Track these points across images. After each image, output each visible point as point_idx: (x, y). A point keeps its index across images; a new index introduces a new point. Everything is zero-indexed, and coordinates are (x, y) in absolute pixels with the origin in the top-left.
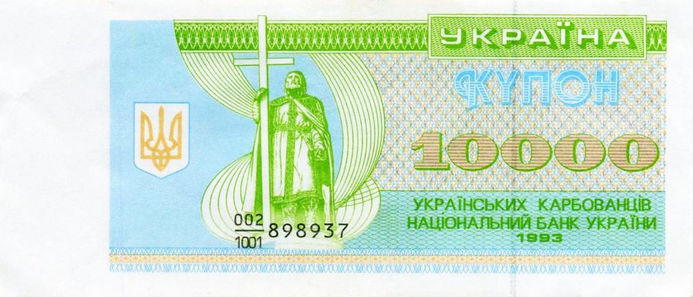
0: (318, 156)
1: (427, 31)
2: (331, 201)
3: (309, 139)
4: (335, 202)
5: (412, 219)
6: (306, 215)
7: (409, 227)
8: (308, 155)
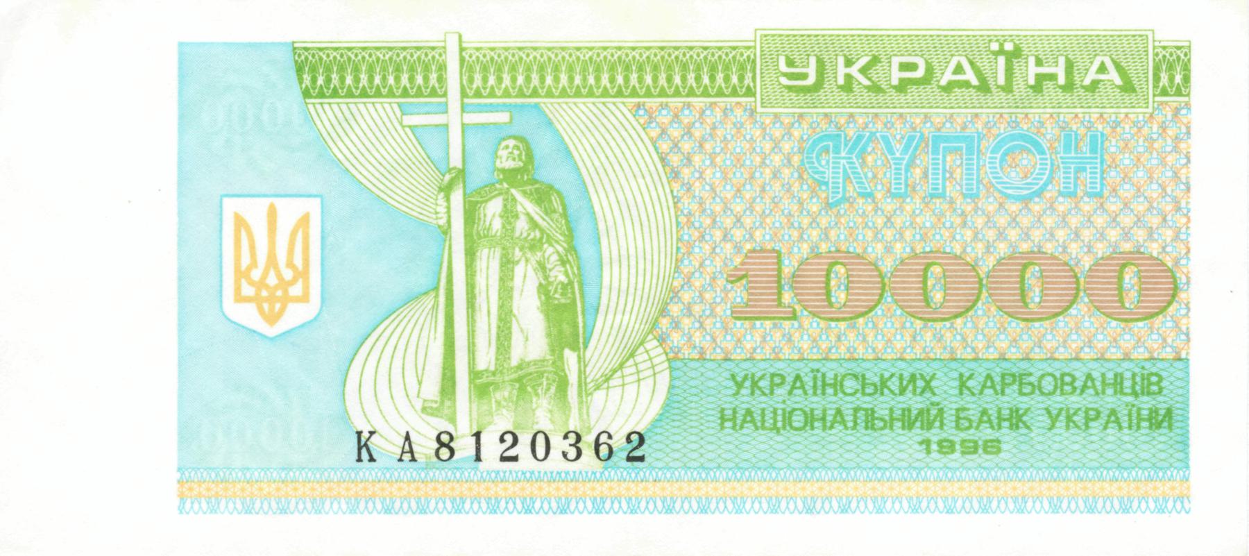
0: (557, 296)
1: (754, 61)
2: (580, 377)
3: (539, 263)
4: (589, 380)
5: (728, 413)
6: (534, 406)
7: (722, 428)
8: (539, 292)
